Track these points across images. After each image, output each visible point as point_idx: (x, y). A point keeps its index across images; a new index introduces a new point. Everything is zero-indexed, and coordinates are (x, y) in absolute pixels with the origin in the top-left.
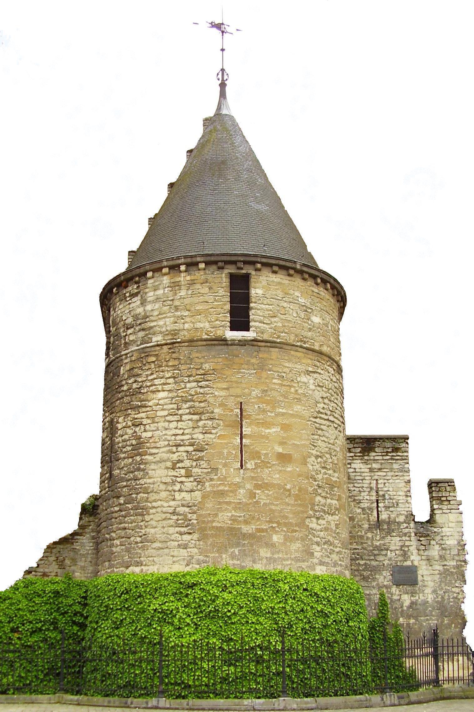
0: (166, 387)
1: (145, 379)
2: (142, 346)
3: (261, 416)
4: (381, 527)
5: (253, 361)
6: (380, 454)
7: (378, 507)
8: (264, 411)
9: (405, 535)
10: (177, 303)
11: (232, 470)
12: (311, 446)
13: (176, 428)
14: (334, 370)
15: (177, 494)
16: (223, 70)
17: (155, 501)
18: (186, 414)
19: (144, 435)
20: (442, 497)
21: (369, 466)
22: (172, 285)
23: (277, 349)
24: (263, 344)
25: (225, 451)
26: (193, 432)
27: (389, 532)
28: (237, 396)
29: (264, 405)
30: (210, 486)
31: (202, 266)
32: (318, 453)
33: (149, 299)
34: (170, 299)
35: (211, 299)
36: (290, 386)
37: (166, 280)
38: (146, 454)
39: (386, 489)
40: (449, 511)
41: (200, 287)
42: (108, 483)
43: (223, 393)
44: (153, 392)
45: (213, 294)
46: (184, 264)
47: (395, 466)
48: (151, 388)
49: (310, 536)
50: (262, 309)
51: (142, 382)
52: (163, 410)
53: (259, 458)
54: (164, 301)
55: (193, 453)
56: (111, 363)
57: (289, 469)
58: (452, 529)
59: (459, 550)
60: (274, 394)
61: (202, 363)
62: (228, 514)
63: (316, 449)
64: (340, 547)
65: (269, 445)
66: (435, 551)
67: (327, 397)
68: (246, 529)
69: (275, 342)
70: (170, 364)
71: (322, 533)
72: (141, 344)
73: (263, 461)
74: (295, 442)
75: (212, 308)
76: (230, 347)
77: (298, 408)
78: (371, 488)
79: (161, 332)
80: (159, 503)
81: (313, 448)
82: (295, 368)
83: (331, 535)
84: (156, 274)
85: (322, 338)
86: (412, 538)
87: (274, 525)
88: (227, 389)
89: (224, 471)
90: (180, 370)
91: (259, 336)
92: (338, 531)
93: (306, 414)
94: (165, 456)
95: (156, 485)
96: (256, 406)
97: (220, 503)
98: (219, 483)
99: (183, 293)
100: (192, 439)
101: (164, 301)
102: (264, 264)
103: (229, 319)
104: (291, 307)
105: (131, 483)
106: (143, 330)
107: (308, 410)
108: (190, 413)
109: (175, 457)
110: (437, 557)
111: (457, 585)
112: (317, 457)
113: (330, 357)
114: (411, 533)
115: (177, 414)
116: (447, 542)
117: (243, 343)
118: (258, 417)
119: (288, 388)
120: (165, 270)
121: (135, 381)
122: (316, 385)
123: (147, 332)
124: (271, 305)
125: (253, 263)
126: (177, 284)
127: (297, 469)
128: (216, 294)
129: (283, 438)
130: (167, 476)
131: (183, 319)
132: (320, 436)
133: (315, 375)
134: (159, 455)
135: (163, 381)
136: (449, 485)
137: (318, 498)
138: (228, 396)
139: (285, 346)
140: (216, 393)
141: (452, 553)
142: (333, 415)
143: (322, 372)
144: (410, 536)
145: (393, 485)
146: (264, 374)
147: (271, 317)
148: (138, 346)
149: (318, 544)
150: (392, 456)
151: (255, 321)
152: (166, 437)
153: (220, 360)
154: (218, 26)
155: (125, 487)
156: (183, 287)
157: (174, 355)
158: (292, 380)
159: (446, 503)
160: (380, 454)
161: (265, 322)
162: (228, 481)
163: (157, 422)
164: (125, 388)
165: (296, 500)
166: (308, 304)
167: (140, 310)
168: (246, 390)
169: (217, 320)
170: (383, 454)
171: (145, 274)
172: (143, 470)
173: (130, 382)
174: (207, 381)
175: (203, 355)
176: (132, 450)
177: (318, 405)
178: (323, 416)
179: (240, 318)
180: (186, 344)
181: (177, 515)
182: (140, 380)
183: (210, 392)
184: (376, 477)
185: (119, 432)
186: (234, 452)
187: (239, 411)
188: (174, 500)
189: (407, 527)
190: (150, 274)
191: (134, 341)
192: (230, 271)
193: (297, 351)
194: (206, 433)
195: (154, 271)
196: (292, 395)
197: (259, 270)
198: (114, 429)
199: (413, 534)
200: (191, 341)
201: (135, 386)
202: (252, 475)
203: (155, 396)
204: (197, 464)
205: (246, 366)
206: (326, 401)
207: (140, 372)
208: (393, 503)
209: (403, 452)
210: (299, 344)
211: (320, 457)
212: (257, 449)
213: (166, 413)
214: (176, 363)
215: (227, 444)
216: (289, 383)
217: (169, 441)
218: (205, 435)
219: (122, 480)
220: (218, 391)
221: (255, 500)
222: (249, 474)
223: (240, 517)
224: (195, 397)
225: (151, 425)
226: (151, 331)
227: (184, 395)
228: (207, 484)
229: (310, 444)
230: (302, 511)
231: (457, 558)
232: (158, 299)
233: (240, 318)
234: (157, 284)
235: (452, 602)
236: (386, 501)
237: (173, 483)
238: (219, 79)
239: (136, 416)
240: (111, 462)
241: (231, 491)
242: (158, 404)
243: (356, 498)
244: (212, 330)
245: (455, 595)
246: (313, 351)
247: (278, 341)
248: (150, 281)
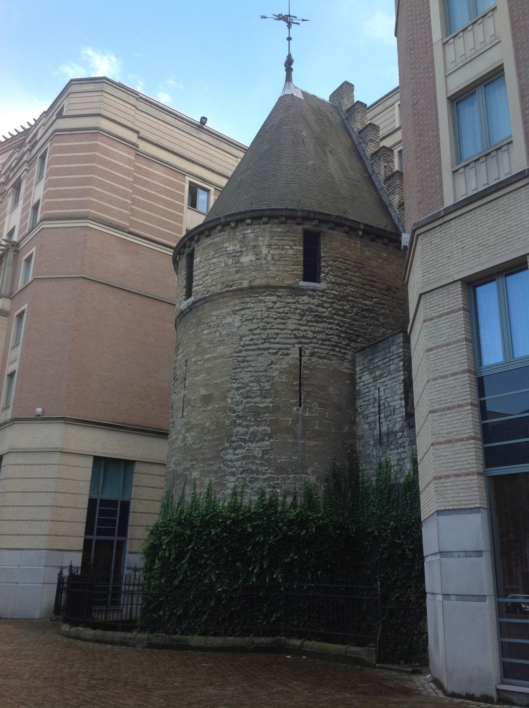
7: (380, 418)
12: (231, 380)
14: (278, 296)
16: (289, 56)
21: (373, 375)
23: (209, 303)
32: (240, 385)
36: (215, 332)
49: (225, 468)
57: (210, 408)
63: (238, 381)
64: (271, 473)
67: (258, 327)
69: (205, 298)
71: (239, 463)
74: (216, 381)
78: (375, 399)
81: (234, 381)
82: (222, 313)
83: (253, 463)
85: (254, 274)
92: (266, 457)
104: (220, 260)
107: (230, 348)
112: (238, 389)
113: (267, 287)
114: (404, 442)
119: (214, 334)
122: (244, 320)
127: (217, 406)
132: (243, 368)
133: (242, 312)
139: (213, 298)
142: (270, 343)
143: (253, 305)
149: (233, 474)
154: (287, 19)
158: (218, 325)
165: (213, 436)
166: (238, 247)
177: (244, 339)
178: (250, 347)
184: (378, 386)
196: (217, 339)
206: (259, 331)
210: (224, 290)
211: (243, 388)
216: (215, 329)
222: (185, 420)
229: (231, 378)
230: (217, 444)
243: (365, 413)
246: (242, 290)
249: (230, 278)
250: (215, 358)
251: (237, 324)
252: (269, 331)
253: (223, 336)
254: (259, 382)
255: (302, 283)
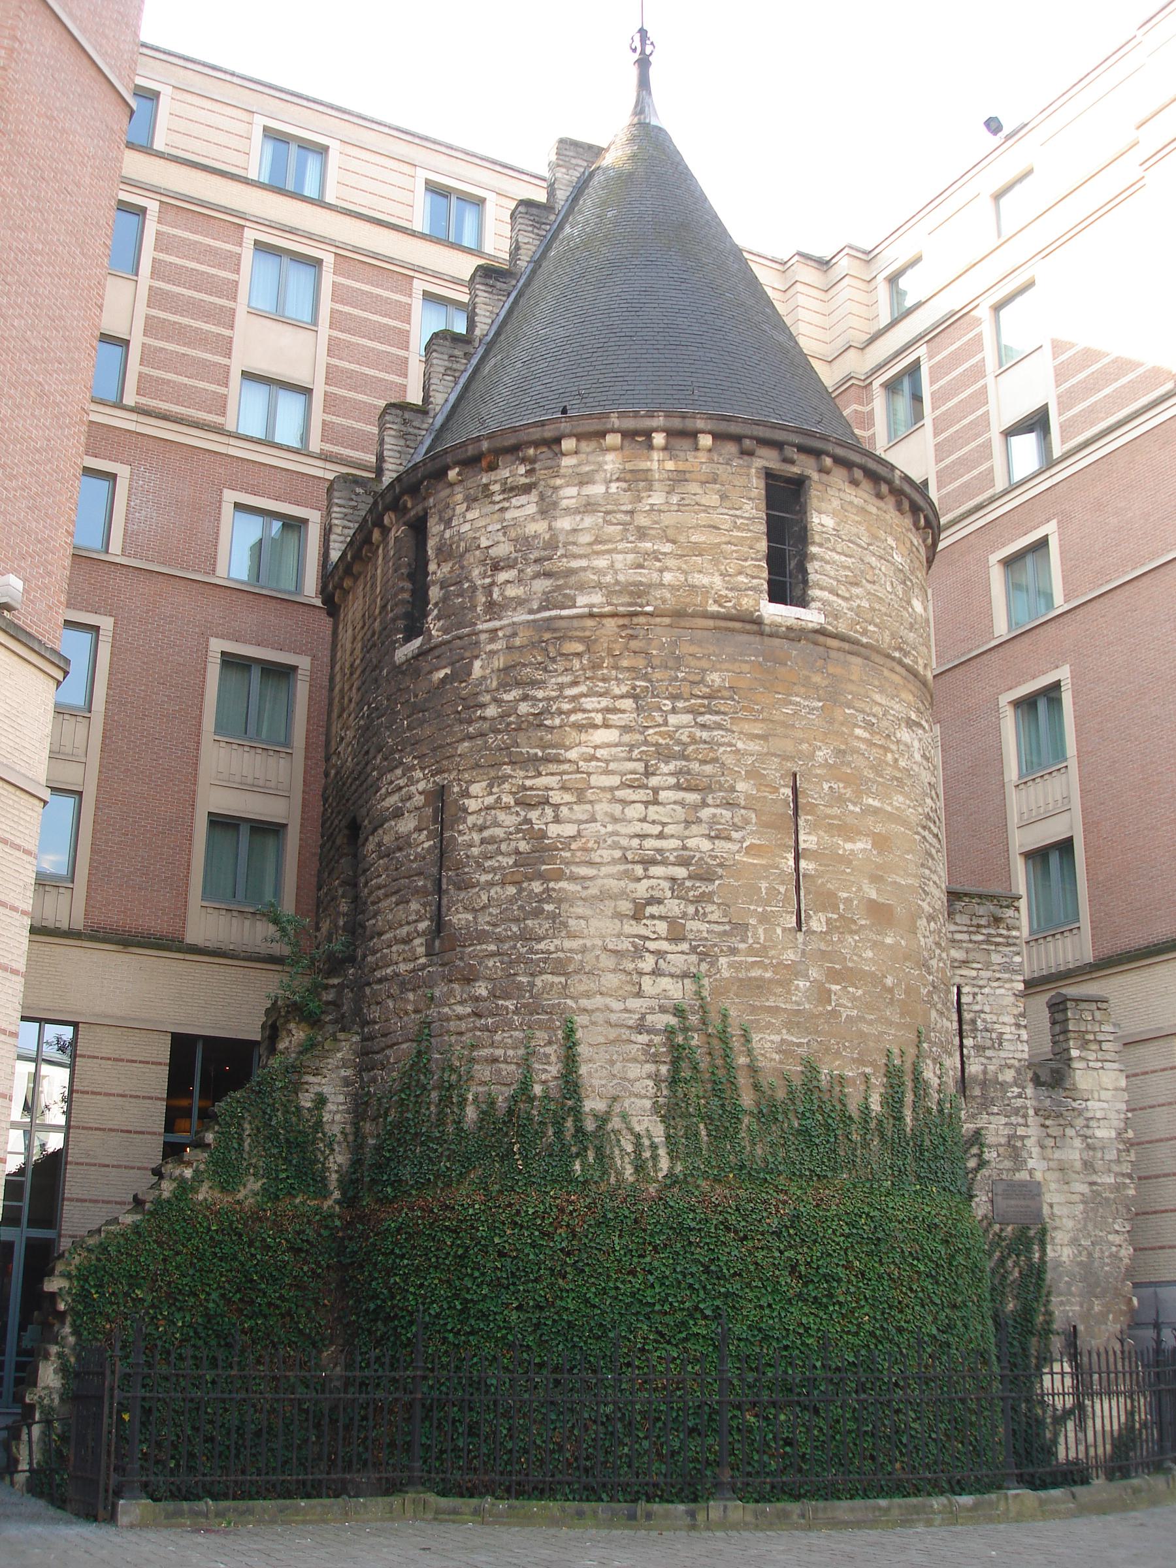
0: (613, 718)
1: (554, 694)
2: (547, 614)
3: (836, 811)
4: (968, 1093)
5: (817, 679)
6: (965, 929)
7: (961, 1046)
8: (840, 800)
9: (1016, 1112)
10: (642, 520)
11: (779, 931)
13: (643, 820)
15: (647, 982)
17: (588, 995)
18: (669, 788)
19: (553, 830)
20: (1087, 1032)
22: (629, 476)
23: (859, 660)
24: (835, 643)
25: (764, 885)
26: (687, 833)
27: (985, 1104)
28: (785, 758)
29: (841, 785)
30: (730, 965)
31: (706, 441)
33: (564, 503)
34: (624, 508)
35: (725, 521)
36: (886, 749)
37: (611, 462)
38: (559, 876)
39: (977, 1008)
40: (1100, 1064)
41: (700, 491)
42: (429, 946)
43: (754, 746)
44: (579, 727)
45: (731, 512)
46: (663, 431)
47: (996, 958)
48: (573, 718)
50: (834, 562)
51: (548, 699)
52: (607, 772)
53: (835, 909)
54: (607, 513)
55: (688, 884)
56: (432, 649)
58: (1105, 1105)
59: (1119, 1150)
60: (860, 762)
61: (704, 671)
62: (772, 1037)
65: (852, 879)
66: (1074, 1153)
69: (856, 642)
70: (625, 663)
72: (539, 610)
73: (841, 916)
74: (898, 880)
75: (729, 543)
76: (766, 639)
77: (899, 800)
79: (599, 586)
80: (598, 1001)
84: (585, 446)
86: (1030, 1120)
87: (868, 1070)
88: (764, 737)
89: (761, 931)
90: (650, 681)
91: (829, 624)
94: (614, 885)
95: (589, 957)
96: (826, 786)
97: (754, 1009)
98: (750, 959)
99: (657, 498)
100: (684, 848)
101: (607, 513)
102: (839, 461)
103: (765, 575)
104: (883, 569)
105: (514, 947)
106: (548, 575)
108: (678, 787)
109: (641, 890)
110: (1078, 1165)
111: (1117, 1227)
115: (646, 787)
116: (1099, 1133)
117: (795, 634)
118: (829, 811)
119: (881, 751)
120: (613, 439)
121: (525, 698)
123: (561, 582)
124: (850, 556)
125: (817, 453)
126: (643, 477)
128: (738, 513)
129: (879, 867)
130: (618, 936)
131: (659, 560)
134: (600, 882)
135: (605, 702)
136: (1099, 1009)
138: (767, 754)
140: (740, 745)
141: (1107, 1157)
144: (1025, 1116)
145: (991, 998)
146: (838, 714)
147: (851, 583)
148: (531, 612)
150: (989, 935)
151: (821, 589)
152: (616, 838)
153: (746, 668)
155: (492, 955)
156: (656, 485)
157: (634, 644)
159: (1094, 1047)
160: (965, 929)
161: (840, 592)
162: (773, 957)
163: (591, 802)
164: (491, 711)
165: (902, 1015)
167: (538, 527)
168: (805, 746)
169: (740, 573)
170: (971, 929)
171: (558, 441)
172: (553, 917)
173: (506, 697)
174: (717, 713)
175: (706, 652)
176: (516, 864)
179: (786, 578)
180: (667, 620)
181: (649, 1032)
182: (540, 694)
183: (726, 740)
184: (957, 980)
185: (471, 820)
186: (782, 890)
187: (788, 791)
188: (639, 994)
189: (1019, 1096)
190: (568, 444)
191: (520, 602)
192: (767, 464)
193: (892, 670)
194: (717, 837)
195: (579, 437)
197: (828, 472)
198: (450, 811)
199: (1031, 1112)
200: (679, 614)
201: (524, 708)
202: (823, 946)
203: (584, 737)
204: (697, 910)
205: (803, 690)
207: (539, 675)
208: (991, 1039)
209: (1008, 929)
210: (897, 654)
212: (829, 885)
213: (615, 780)
214: (640, 662)
215: (766, 867)
217: (625, 849)
218: (716, 842)
219: (482, 937)
220: (741, 743)
221: (829, 1008)
222: (816, 944)
223: (799, 1045)
224: (691, 748)
225: (575, 807)
226: (573, 580)
227: (661, 741)
228: (723, 961)
231: (1116, 1168)
232: (589, 507)
233: (786, 578)
234: (587, 468)
235: (1108, 1265)
236: (979, 1034)
237: (638, 953)
238: (634, 50)
239: (528, 783)
240: (440, 891)
241: (780, 983)
242: (593, 758)
244: (730, 594)
245: (1114, 1249)
247: (865, 640)
248: (566, 462)
253: (899, 769)
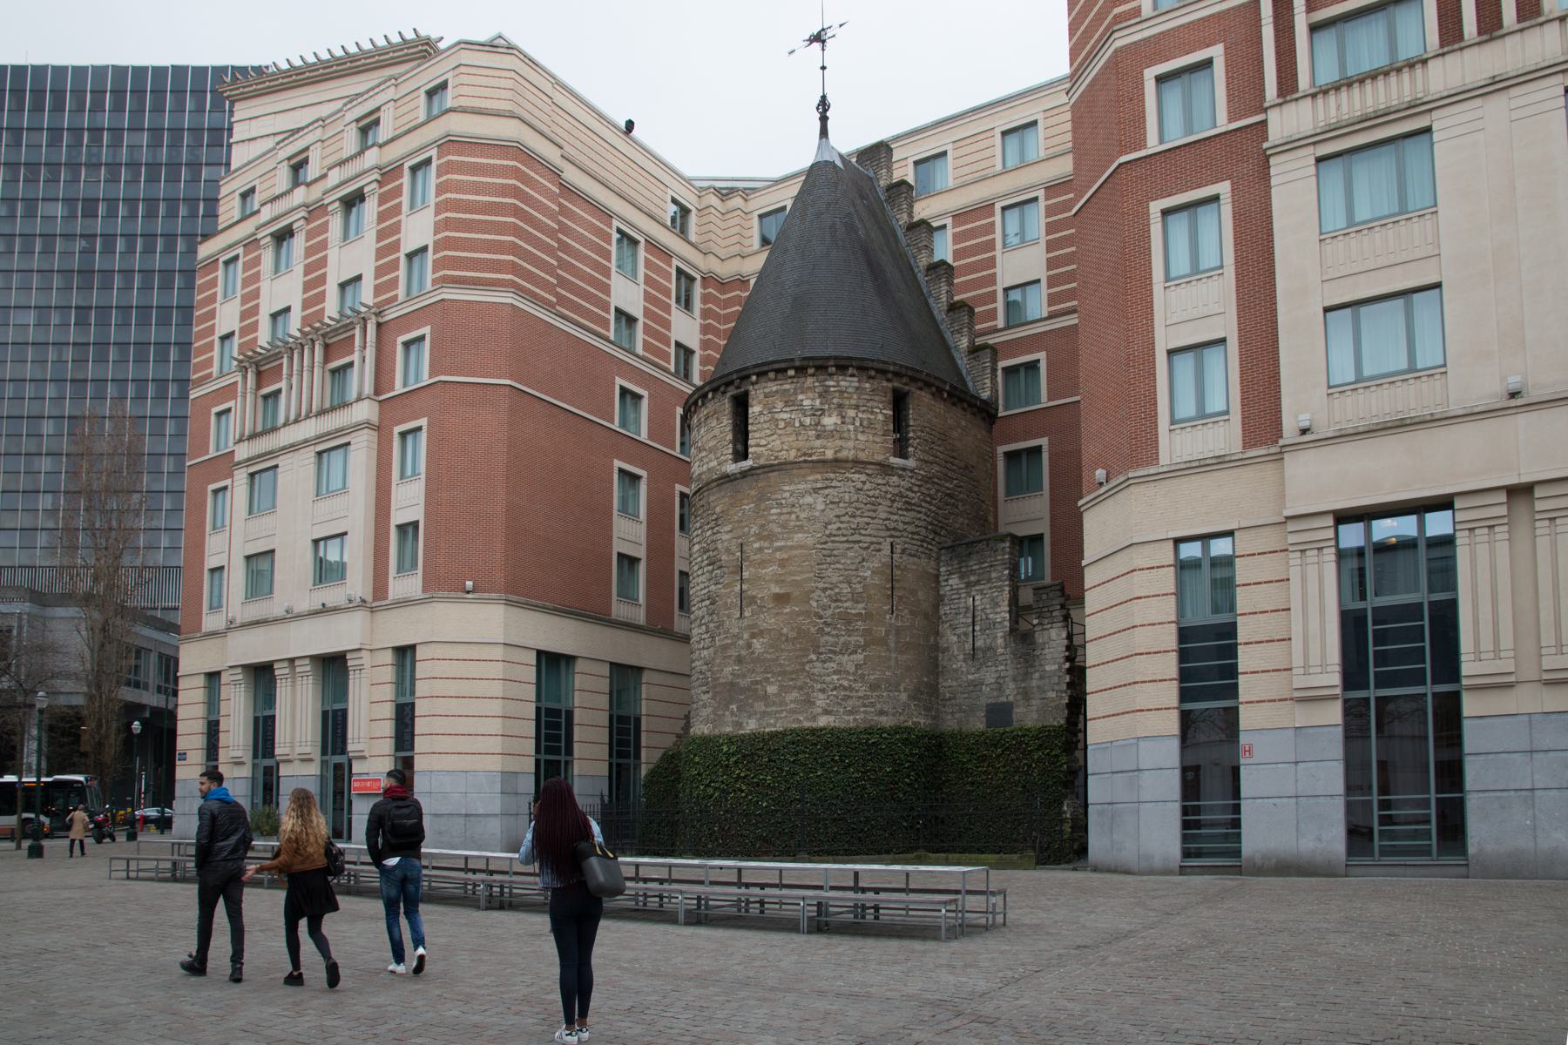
5: (753, 493)
68: (743, 683)
93: (810, 541)
113: (856, 462)
137: (823, 640)
149: (823, 691)
206: (846, 518)
246: (824, 461)
249: (808, 445)
250: (792, 548)
251: (820, 507)
252: (859, 519)
254: (849, 583)
255: (894, 461)
